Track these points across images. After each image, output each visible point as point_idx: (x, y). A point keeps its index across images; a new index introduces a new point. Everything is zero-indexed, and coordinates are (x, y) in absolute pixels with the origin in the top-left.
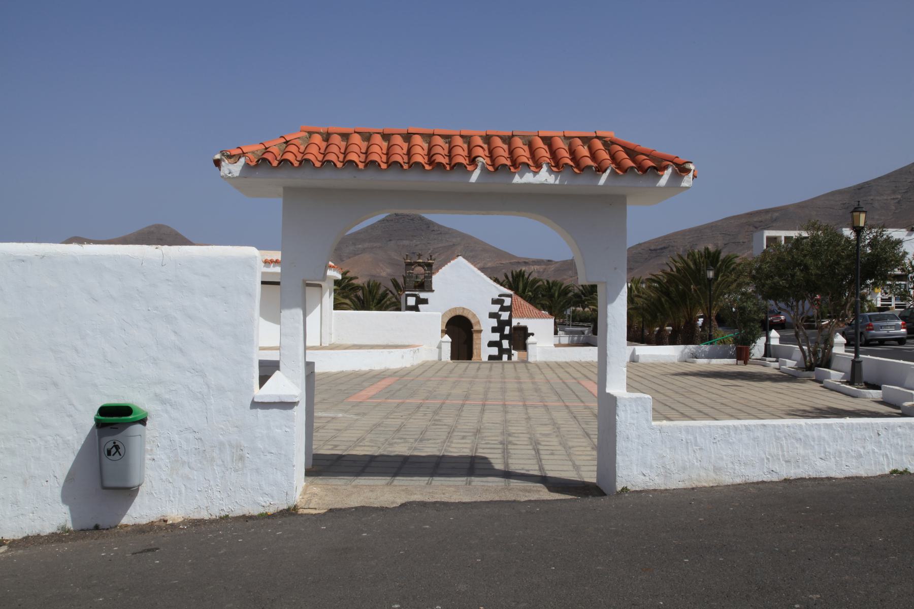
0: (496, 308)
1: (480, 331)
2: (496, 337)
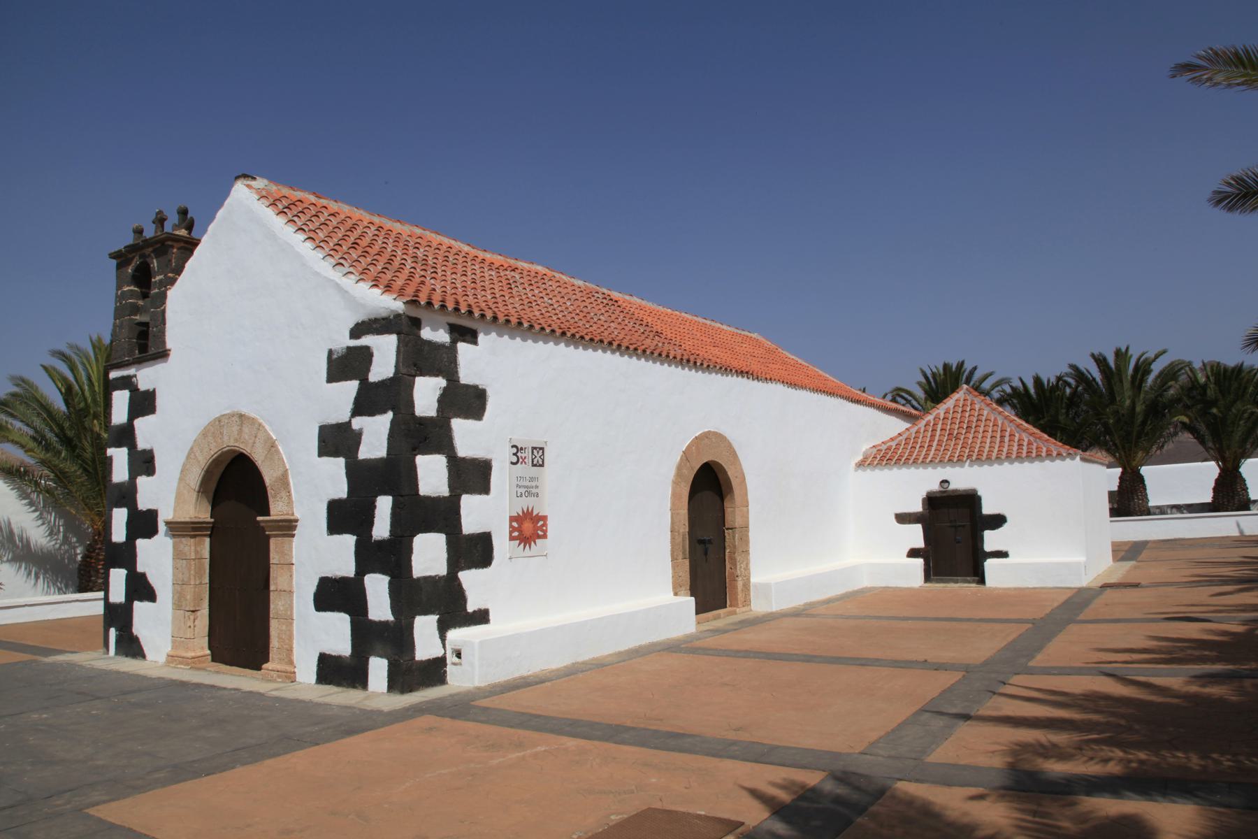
1: (288, 527)
2: (339, 556)
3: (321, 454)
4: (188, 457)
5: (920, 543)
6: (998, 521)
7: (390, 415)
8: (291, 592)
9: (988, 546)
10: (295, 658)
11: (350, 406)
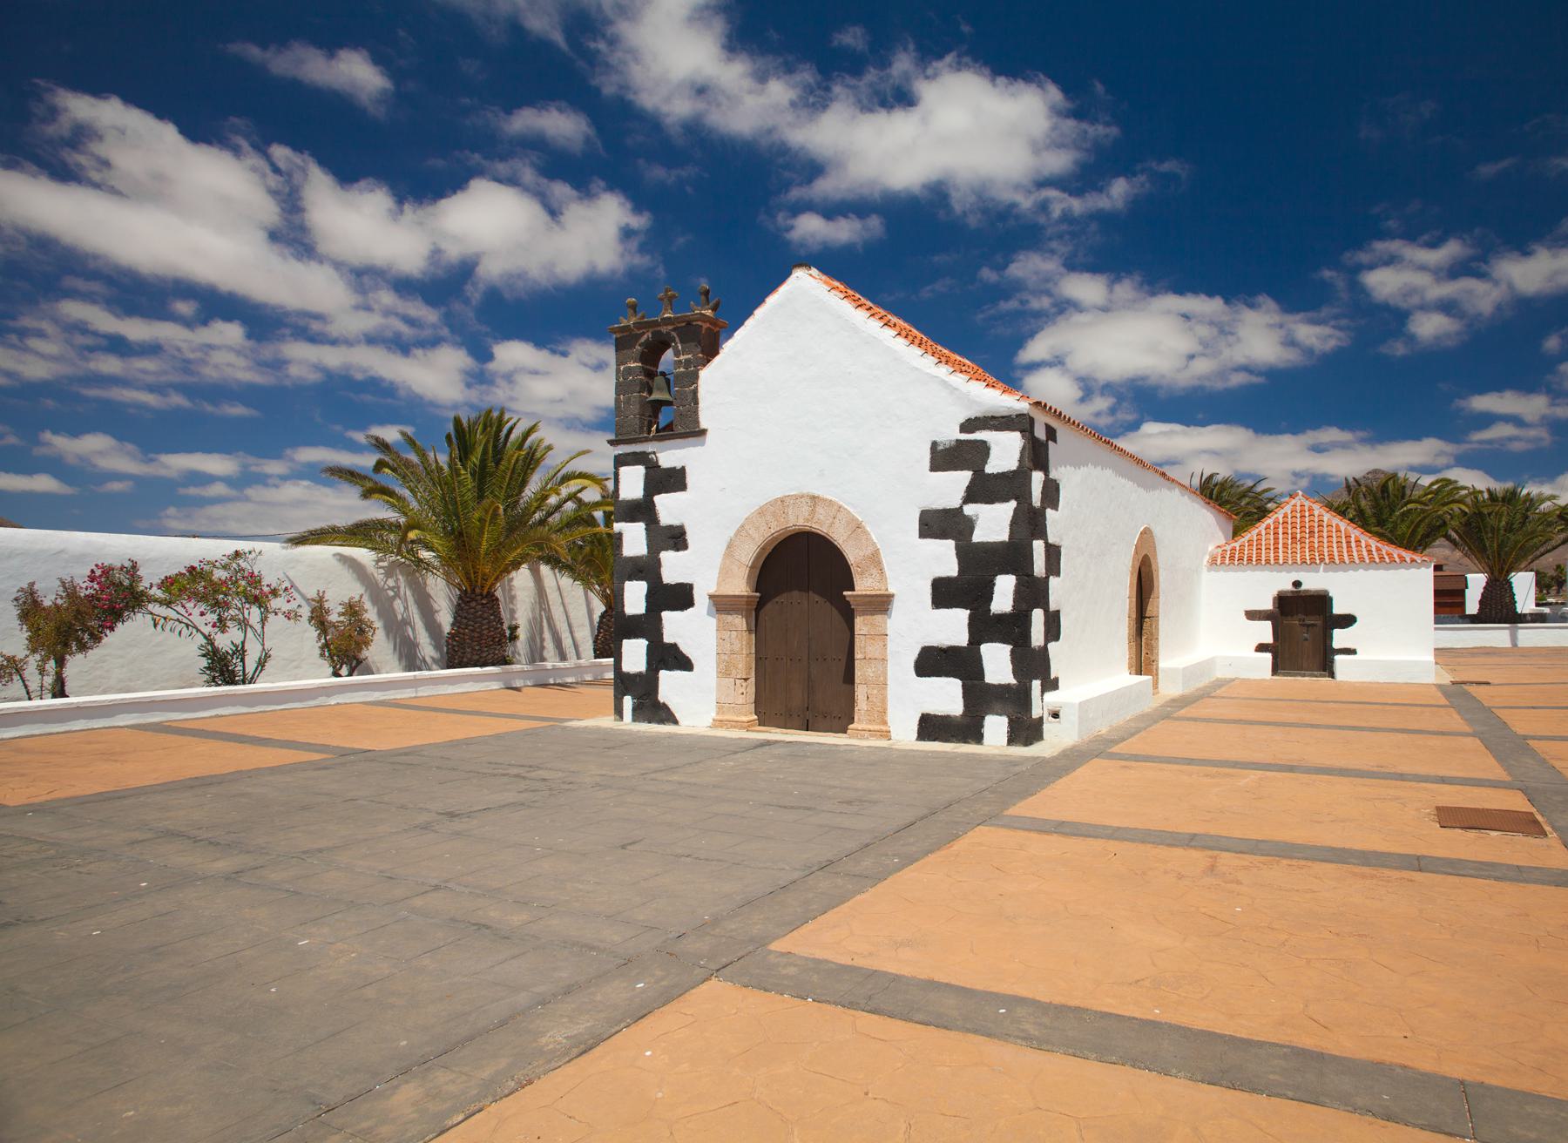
0: (951, 487)
1: (881, 604)
2: (953, 627)
3: (922, 535)
4: (738, 532)
5: (1268, 638)
6: (1348, 621)
7: (1013, 504)
8: (884, 660)
9: (1336, 645)
10: (890, 717)
11: (961, 493)
